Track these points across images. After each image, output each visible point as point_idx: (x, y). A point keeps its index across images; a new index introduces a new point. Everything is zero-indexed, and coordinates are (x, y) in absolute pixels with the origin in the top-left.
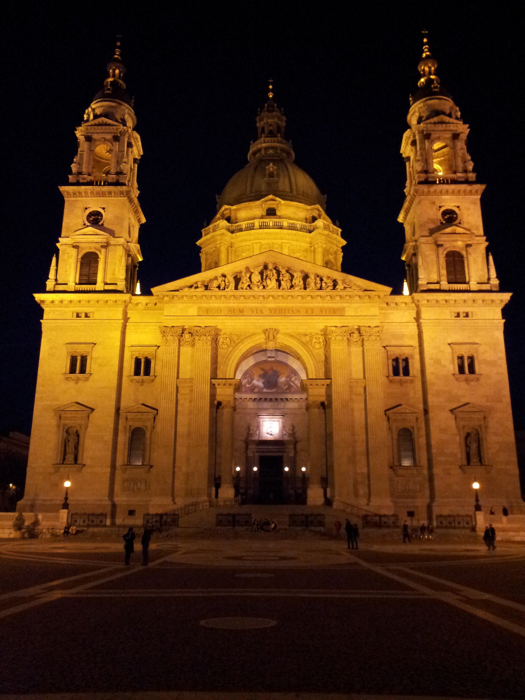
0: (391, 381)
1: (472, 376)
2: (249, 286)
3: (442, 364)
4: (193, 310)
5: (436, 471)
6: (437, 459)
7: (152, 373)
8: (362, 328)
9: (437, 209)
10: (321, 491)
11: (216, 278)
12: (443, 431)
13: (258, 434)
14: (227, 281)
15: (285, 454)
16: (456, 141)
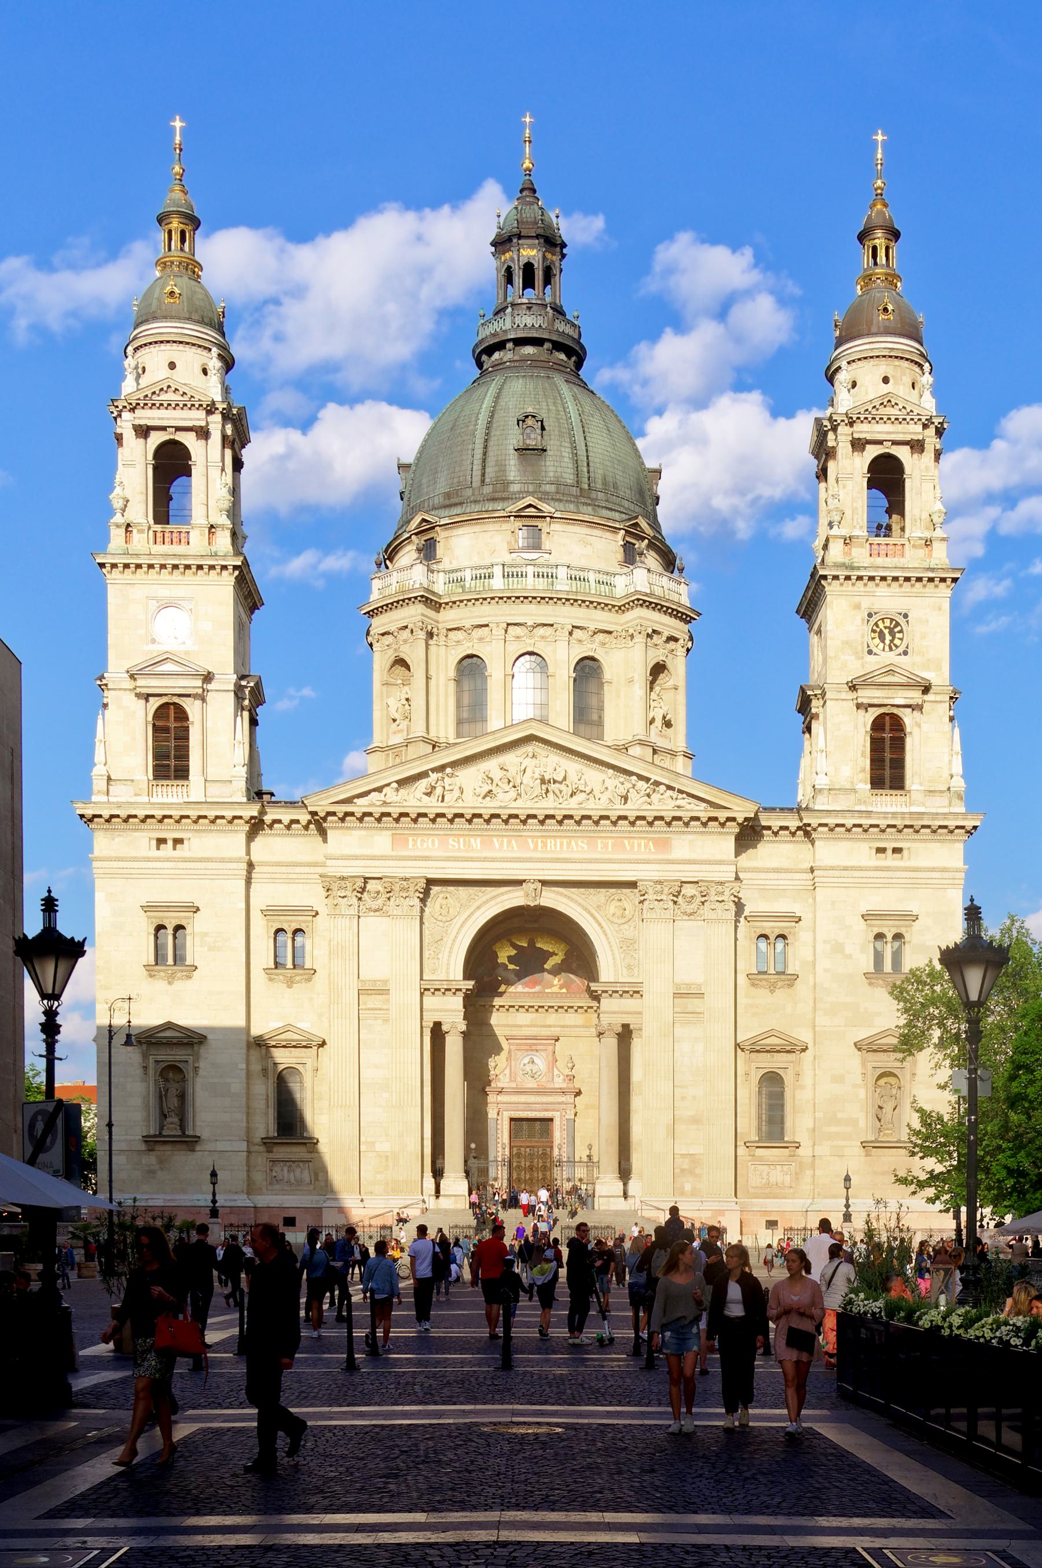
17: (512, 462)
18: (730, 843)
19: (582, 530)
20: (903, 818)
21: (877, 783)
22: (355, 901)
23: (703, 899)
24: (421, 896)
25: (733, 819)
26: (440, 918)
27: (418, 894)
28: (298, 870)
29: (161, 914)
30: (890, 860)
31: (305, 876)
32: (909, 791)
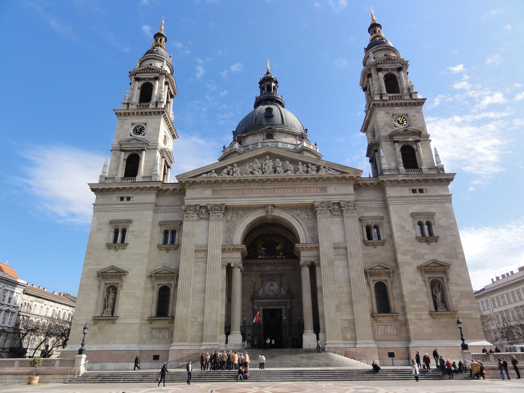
0: (365, 243)
1: (431, 238)
2: (251, 172)
3: (407, 228)
4: (208, 193)
5: (409, 317)
6: (410, 306)
7: (176, 242)
8: (341, 202)
9: (391, 117)
10: (315, 335)
11: (226, 167)
12: (412, 283)
13: (262, 291)
14: (234, 169)
15: (283, 307)
16: (400, 72)
17: (264, 120)
18: (352, 188)
19: (286, 135)
20: (422, 176)
21: (406, 166)
22: (196, 215)
23: (342, 209)
24: (223, 212)
25: (352, 178)
26: (231, 221)
27: (221, 211)
28: (175, 208)
29: (117, 224)
30: (418, 194)
31: (178, 210)
32: (421, 169)
